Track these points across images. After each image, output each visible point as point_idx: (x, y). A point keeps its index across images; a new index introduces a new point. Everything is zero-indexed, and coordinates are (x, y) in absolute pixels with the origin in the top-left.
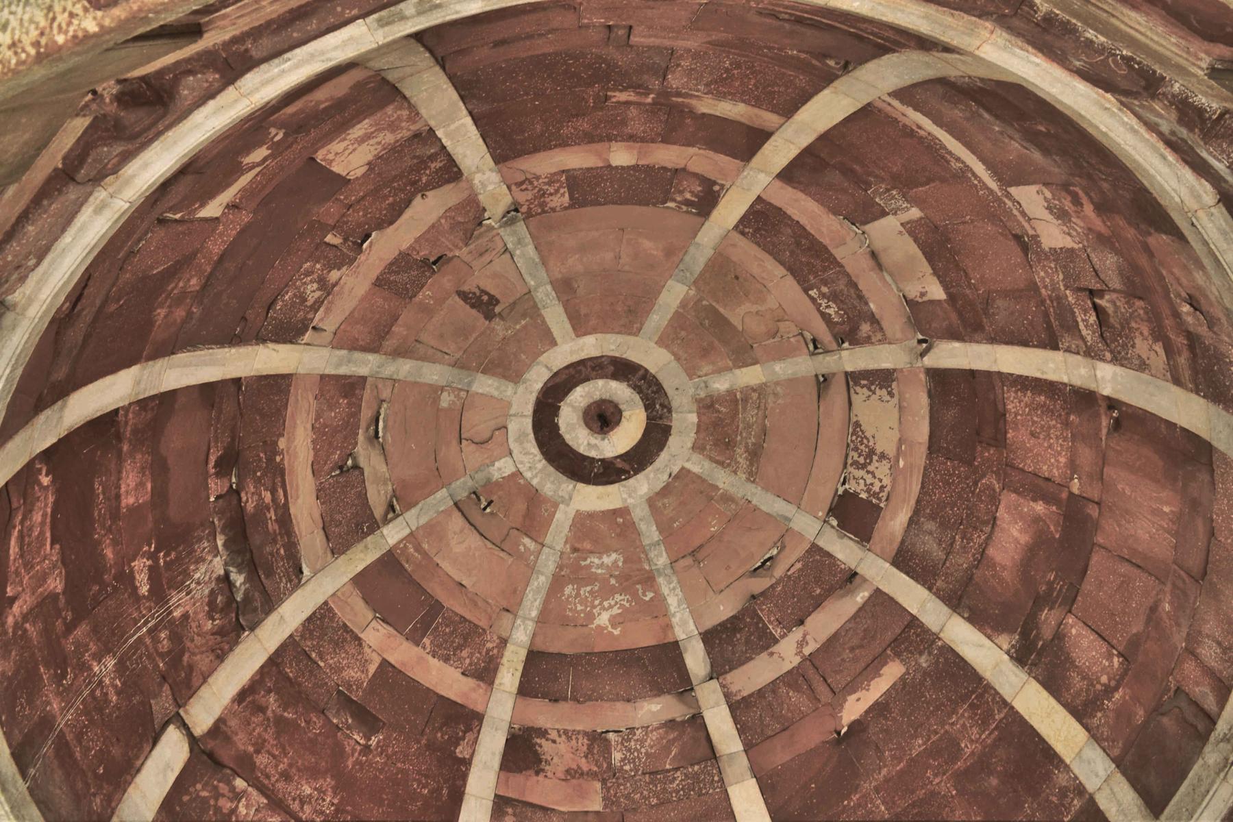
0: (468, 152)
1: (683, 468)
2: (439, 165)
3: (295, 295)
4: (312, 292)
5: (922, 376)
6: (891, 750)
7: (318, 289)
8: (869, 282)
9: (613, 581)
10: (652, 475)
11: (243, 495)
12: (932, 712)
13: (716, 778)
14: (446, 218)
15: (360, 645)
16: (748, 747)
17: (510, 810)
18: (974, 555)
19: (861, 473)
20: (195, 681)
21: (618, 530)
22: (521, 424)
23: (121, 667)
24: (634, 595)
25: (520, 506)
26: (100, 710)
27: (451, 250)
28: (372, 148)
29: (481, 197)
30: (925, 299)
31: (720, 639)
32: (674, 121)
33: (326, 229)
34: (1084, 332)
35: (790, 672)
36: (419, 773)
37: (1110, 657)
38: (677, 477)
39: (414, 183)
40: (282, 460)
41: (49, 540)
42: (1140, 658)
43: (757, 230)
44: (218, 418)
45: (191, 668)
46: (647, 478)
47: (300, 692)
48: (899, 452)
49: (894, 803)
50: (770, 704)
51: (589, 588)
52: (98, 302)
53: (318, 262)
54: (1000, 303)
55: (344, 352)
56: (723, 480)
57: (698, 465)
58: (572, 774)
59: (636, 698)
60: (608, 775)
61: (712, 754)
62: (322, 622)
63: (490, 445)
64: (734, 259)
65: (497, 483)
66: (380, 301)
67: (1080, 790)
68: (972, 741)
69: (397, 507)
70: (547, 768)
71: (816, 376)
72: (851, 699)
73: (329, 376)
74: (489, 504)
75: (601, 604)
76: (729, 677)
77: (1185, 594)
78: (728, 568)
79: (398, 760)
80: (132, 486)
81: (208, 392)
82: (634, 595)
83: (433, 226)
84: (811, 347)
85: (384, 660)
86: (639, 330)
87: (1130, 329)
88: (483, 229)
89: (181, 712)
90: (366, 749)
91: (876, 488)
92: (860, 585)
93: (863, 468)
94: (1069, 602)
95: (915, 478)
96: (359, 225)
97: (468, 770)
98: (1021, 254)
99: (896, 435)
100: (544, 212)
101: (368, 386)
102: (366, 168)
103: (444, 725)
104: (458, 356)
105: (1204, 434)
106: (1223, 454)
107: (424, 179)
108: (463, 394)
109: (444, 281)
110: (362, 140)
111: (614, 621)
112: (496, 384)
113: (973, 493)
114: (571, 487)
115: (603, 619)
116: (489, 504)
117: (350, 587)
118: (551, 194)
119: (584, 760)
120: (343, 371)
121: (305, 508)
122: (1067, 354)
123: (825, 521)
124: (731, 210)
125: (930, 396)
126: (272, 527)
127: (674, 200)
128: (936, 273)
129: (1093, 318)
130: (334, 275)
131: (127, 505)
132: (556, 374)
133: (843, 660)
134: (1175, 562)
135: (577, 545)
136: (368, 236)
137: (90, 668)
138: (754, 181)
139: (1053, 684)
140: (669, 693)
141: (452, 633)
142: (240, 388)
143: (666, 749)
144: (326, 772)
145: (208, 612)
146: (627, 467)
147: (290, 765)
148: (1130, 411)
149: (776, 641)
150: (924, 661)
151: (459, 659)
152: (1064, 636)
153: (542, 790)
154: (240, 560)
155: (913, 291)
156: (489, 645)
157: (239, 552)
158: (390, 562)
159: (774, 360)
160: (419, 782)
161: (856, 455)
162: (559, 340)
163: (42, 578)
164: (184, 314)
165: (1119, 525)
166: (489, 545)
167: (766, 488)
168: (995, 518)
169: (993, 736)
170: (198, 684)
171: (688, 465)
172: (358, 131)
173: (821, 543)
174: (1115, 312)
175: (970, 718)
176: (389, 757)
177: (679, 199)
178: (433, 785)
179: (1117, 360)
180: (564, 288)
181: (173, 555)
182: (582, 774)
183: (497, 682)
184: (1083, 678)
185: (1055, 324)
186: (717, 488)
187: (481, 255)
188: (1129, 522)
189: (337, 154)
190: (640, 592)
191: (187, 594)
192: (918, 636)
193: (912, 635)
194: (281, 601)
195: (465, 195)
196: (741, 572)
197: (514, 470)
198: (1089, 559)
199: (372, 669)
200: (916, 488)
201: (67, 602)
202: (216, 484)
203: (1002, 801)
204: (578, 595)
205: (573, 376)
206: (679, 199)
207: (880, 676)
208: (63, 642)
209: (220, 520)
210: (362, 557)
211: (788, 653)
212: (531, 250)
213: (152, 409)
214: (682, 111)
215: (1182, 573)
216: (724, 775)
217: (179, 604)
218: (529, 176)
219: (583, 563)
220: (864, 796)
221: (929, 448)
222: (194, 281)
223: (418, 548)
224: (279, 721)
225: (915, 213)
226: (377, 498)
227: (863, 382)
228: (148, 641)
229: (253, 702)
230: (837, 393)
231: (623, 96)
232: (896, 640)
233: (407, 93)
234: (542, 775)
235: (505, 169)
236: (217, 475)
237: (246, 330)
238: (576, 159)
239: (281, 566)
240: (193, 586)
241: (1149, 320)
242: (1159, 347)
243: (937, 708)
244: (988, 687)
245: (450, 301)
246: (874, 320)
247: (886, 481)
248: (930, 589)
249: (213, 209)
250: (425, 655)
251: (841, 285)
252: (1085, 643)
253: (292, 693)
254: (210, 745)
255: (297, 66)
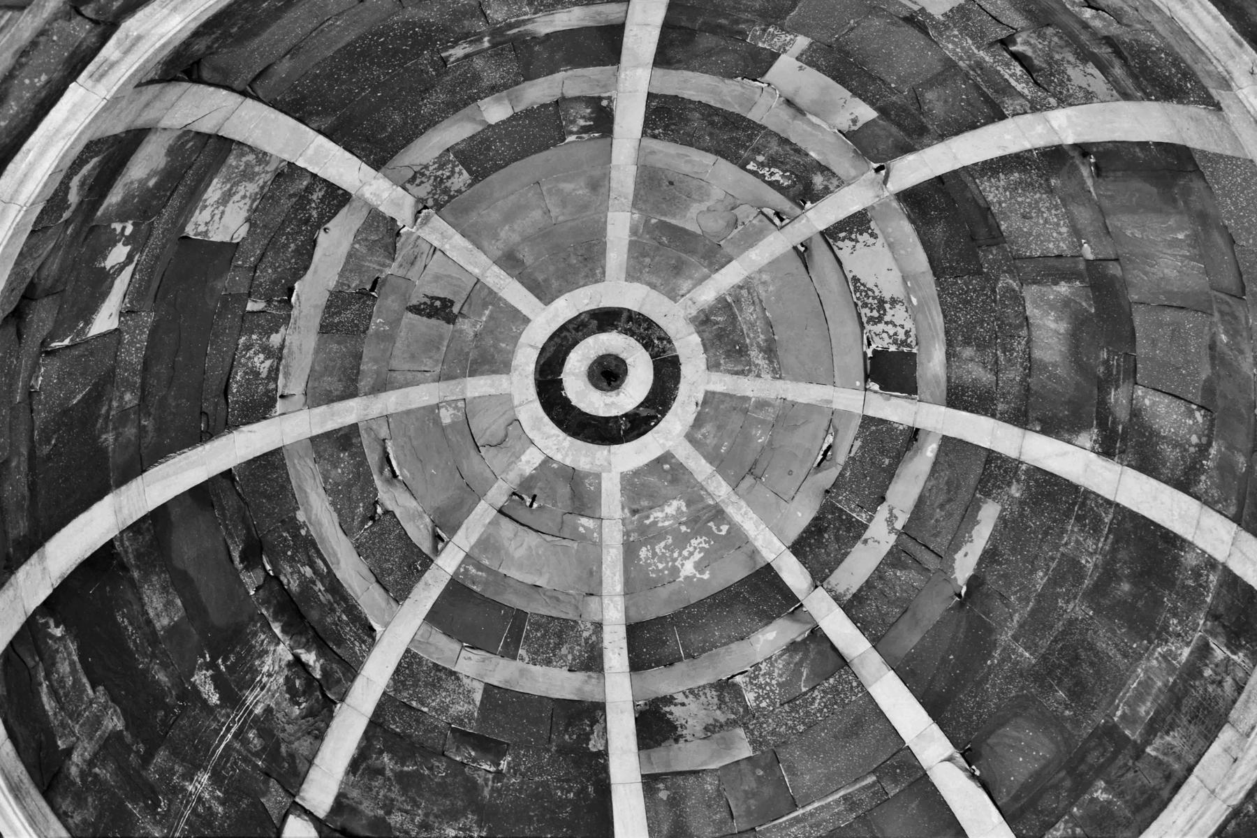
0: (341, 170)
1: (707, 392)
2: (321, 194)
3: (246, 373)
4: (263, 364)
5: (895, 204)
6: (1015, 593)
7: (266, 358)
8: (797, 132)
9: (683, 528)
10: (679, 411)
11: (282, 578)
12: (1042, 540)
13: (855, 684)
14: (358, 242)
15: (458, 679)
16: (876, 642)
17: (661, 786)
18: (1022, 364)
19: (881, 327)
20: (301, 767)
21: (669, 477)
22: (531, 411)
23: (216, 778)
24: (709, 533)
25: (564, 490)
26: (209, 825)
27: (381, 271)
28: (241, 204)
29: (381, 209)
30: (859, 124)
31: (810, 545)
32: (529, 56)
33: (242, 299)
34: (1019, 87)
35: (890, 553)
36: (559, 780)
37: (1190, 414)
38: (705, 402)
39: (307, 222)
40: (308, 531)
41: (88, 686)
42: (1220, 402)
43: (666, 128)
44: (223, 515)
45: (292, 756)
46: (676, 415)
47: (413, 744)
48: (908, 291)
49: (1036, 645)
50: (882, 592)
51: (662, 544)
52: (24, 451)
53: (253, 333)
54: (930, 96)
55: (324, 408)
56: (748, 387)
57: (722, 383)
58: (710, 729)
59: (748, 634)
60: (746, 718)
61: (842, 661)
62: (411, 670)
63: (509, 442)
64: (659, 165)
65: (531, 477)
66: (335, 347)
67: (1212, 563)
68: (1091, 555)
69: (443, 535)
70: (684, 732)
71: (795, 248)
72: (959, 556)
73: (318, 436)
74: (534, 498)
75: (680, 554)
76: (833, 580)
77: (1236, 318)
78: (790, 473)
79: (534, 774)
80: (160, 608)
81: (201, 495)
82: (709, 533)
83: (350, 255)
84: (777, 221)
85: (487, 684)
86: (604, 273)
87: (1056, 62)
88: (403, 239)
89: (297, 800)
90: (499, 775)
91: (902, 336)
92: (925, 440)
93: (880, 322)
94: (1131, 373)
95: (933, 308)
96: (274, 282)
97: (607, 760)
98: (920, 35)
99: (896, 275)
100: (451, 197)
101: (362, 432)
102: (247, 226)
103: (568, 725)
104: (438, 369)
105: (1176, 140)
106: (1203, 152)
107: (315, 214)
108: (461, 404)
109: (387, 303)
110: (226, 199)
111: (699, 566)
112: (489, 382)
113: (995, 301)
114: (606, 452)
115: (688, 569)
116: (534, 498)
117: (426, 627)
118: (449, 178)
119: (718, 712)
120: (330, 426)
121: (351, 570)
122: (1016, 118)
123: (866, 390)
124: (630, 117)
125: (912, 221)
126: (325, 598)
127: (571, 133)
128: (855, 94)
129: (1018, 69)
130: (275, 339)
131: (163, 628)
132: (543, 349)
133: (937, 521)
134: (1212, 288)
135: (635, 507)
136: (291, 290)
137: (184, 789)
138: (634, 83)
139: (1147, 465)
140: (779, 616)
141: (543, 636)
142: (233, 480)
143: (796, 673)
144: (465, 809)
145: (291, 699)
146: (652, 412)
147: (426, 815)
148: (1101, 149)
149: (865, 527)
150: (1015, 491)
151: (561, 658)
152: (1140, 410)
153: (688, 755)
154: (304, 640)
155: (844, 122)
156: (586, 634)
157: (301, 634)
158: (456, 590)
159: (747, 249)
160: (562, 789)
161: (867, 311)
162: (530, 317)
163: (97, 722)
164: (134, 431)
165: (1146, 273)
166: (549, 538)
167: (796, 379)
168: (1027, 319)
169: (1109, 541)
170: (305, 769)
171: (711, 388)
172: (213, 192)
173: (870, 413)
174: (1035, 52)
175: (1081, 531)
176: (523, 775)
177: (575, 129)
178: (577, 786)
179: (1064, 101)
180: (510, 261)
181: (232, 658)
182: (721, 726)
183: (606, 666)
184: (1175, 447)
185: (989, 92)
186: (746, 399)
187: (412, 264)
188: (1153, 266)
189: (207, 224)
190: (714, 528)
191: (262, 689)
192: (999, 468)
193: (995, 470)
194: (361, 664)
195: (365, 212)
196: (805, 471)
197: (543, 457)
198: (1132, 321)
199: (478, 697)
200: (939, 320)
201: (134, 736)
202: (250, 577)
203: (1140, 604)
204: (654, 554)
205: (561, 345)
206: (575, 129)
207: (978, 523)
208: (144, 773)
209: (267, 609)
210: (427, 593)
211: (881, 534)
212: (458, 239)
213: (148, 529)
214: (525, 42)
215: (1222, 296)
216: (861, 679)
217: (256, 700)
218: (417, 169)
219: (647, 522)
220: (1004, 649)
221: (934, 274)
222: (128, 397)
223: (480, 567)
224: (401, 777)
225: (802, 42)
226: (419, 534)
227: (842, 235)
228: (237, 745)
229: (368, 768)
230: (821, 254)
231: (459, 52)
232: (980, 481)
233: (237, 138)
234: (682, 741)
235: (388, 172)
236: (247, 568)
237: (212, 424)
238: (454, 132)
239: (348, 632)
240: (265, 679)
241: (1068, 45)
242: (1091, 68)
243: (1046, 533)
244: (1087, 492)
245: (405, 321)
246: (823, 169)
247: (909, 325)
248: (993, 416)
249: (105, 320)
250: (526, 666)
251: (774, 147)
252: (1162, 409)
253: (404, 747)
254: (339, 822)
255: (42, 153)
